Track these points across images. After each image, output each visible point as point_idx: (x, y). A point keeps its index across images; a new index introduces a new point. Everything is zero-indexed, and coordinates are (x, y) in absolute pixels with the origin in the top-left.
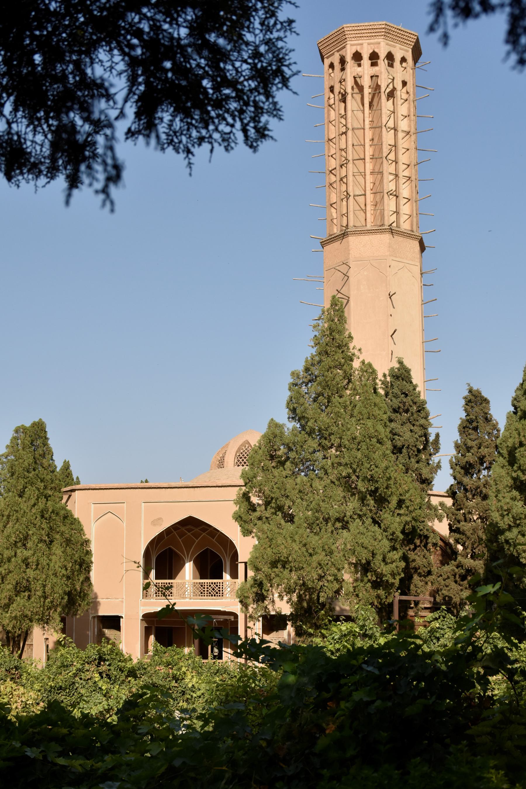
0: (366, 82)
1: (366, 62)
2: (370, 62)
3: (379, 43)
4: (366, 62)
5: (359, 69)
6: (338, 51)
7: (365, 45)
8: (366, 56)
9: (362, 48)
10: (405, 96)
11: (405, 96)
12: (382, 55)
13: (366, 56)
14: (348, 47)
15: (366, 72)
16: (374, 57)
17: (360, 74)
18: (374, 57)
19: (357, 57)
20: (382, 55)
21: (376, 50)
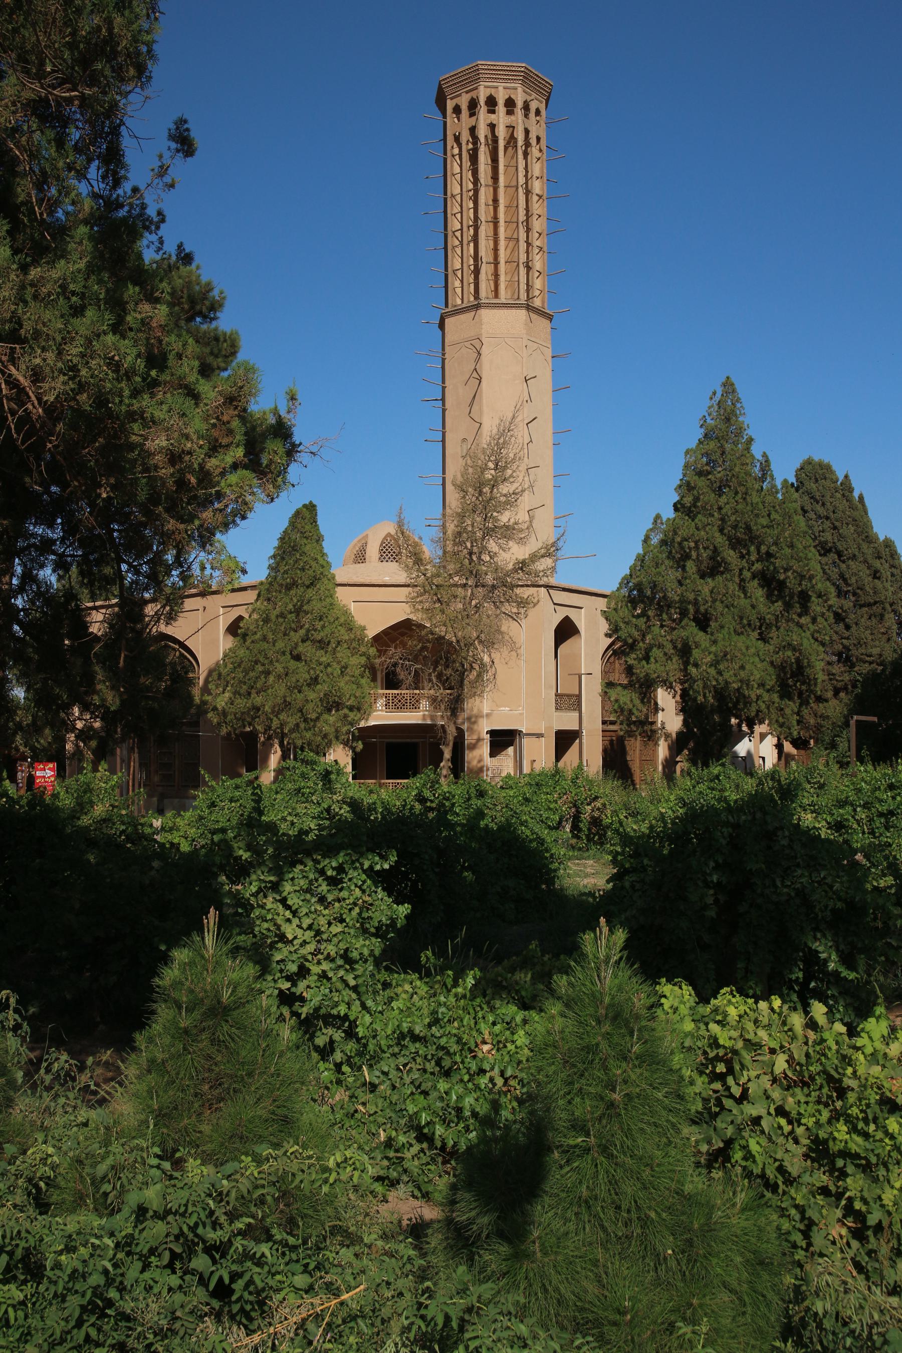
0: (502, 133)
1: (501, 109)
3: (516, 89)
4: (501, 109)
5: (493, 116)
6: (467, 92)
7: (501, 89)
9: (497, 92)
10: (538, 155)
11: (538, 155)
12: (520, 104)
14: (481, 88)
15: (501, 120)
16: (510, 104)
18: (510, 104)
19: (491, 102)
20: (520, 104)
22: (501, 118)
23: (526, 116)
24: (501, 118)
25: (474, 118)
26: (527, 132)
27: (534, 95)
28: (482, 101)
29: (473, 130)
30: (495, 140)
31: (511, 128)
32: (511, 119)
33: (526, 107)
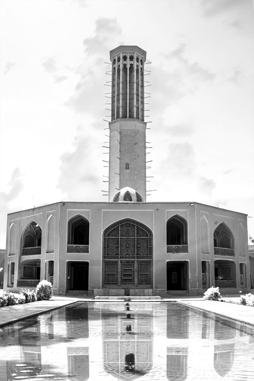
0: (128, 66)
1: (128, 59)
2: (130, 59)
3: (134, 53)
4: (128, 59)
8: (128, 57)
13: (128, 57)
15: (128, 62)
17: (126, 63)
19: (125, 58)
20: (135, 58)
21: (133, 55)
22: (128, 62)
23: (138, 61)
24: (128, 62)
25: (119, 62)
26: (137, 66)
27: (140, 55)
28: (121, 57)
29: (119, 66)
30: (127, 68)
31: (132, 65)
32: (132, 62)
33: (137, 59)
